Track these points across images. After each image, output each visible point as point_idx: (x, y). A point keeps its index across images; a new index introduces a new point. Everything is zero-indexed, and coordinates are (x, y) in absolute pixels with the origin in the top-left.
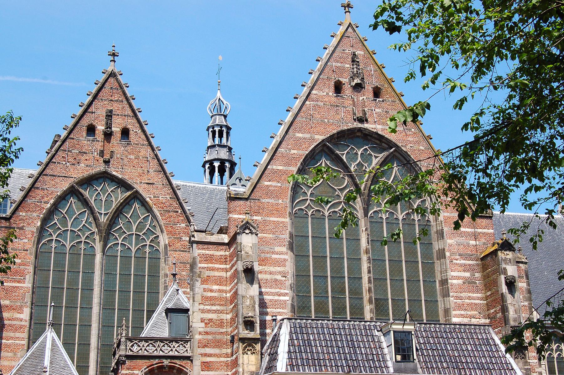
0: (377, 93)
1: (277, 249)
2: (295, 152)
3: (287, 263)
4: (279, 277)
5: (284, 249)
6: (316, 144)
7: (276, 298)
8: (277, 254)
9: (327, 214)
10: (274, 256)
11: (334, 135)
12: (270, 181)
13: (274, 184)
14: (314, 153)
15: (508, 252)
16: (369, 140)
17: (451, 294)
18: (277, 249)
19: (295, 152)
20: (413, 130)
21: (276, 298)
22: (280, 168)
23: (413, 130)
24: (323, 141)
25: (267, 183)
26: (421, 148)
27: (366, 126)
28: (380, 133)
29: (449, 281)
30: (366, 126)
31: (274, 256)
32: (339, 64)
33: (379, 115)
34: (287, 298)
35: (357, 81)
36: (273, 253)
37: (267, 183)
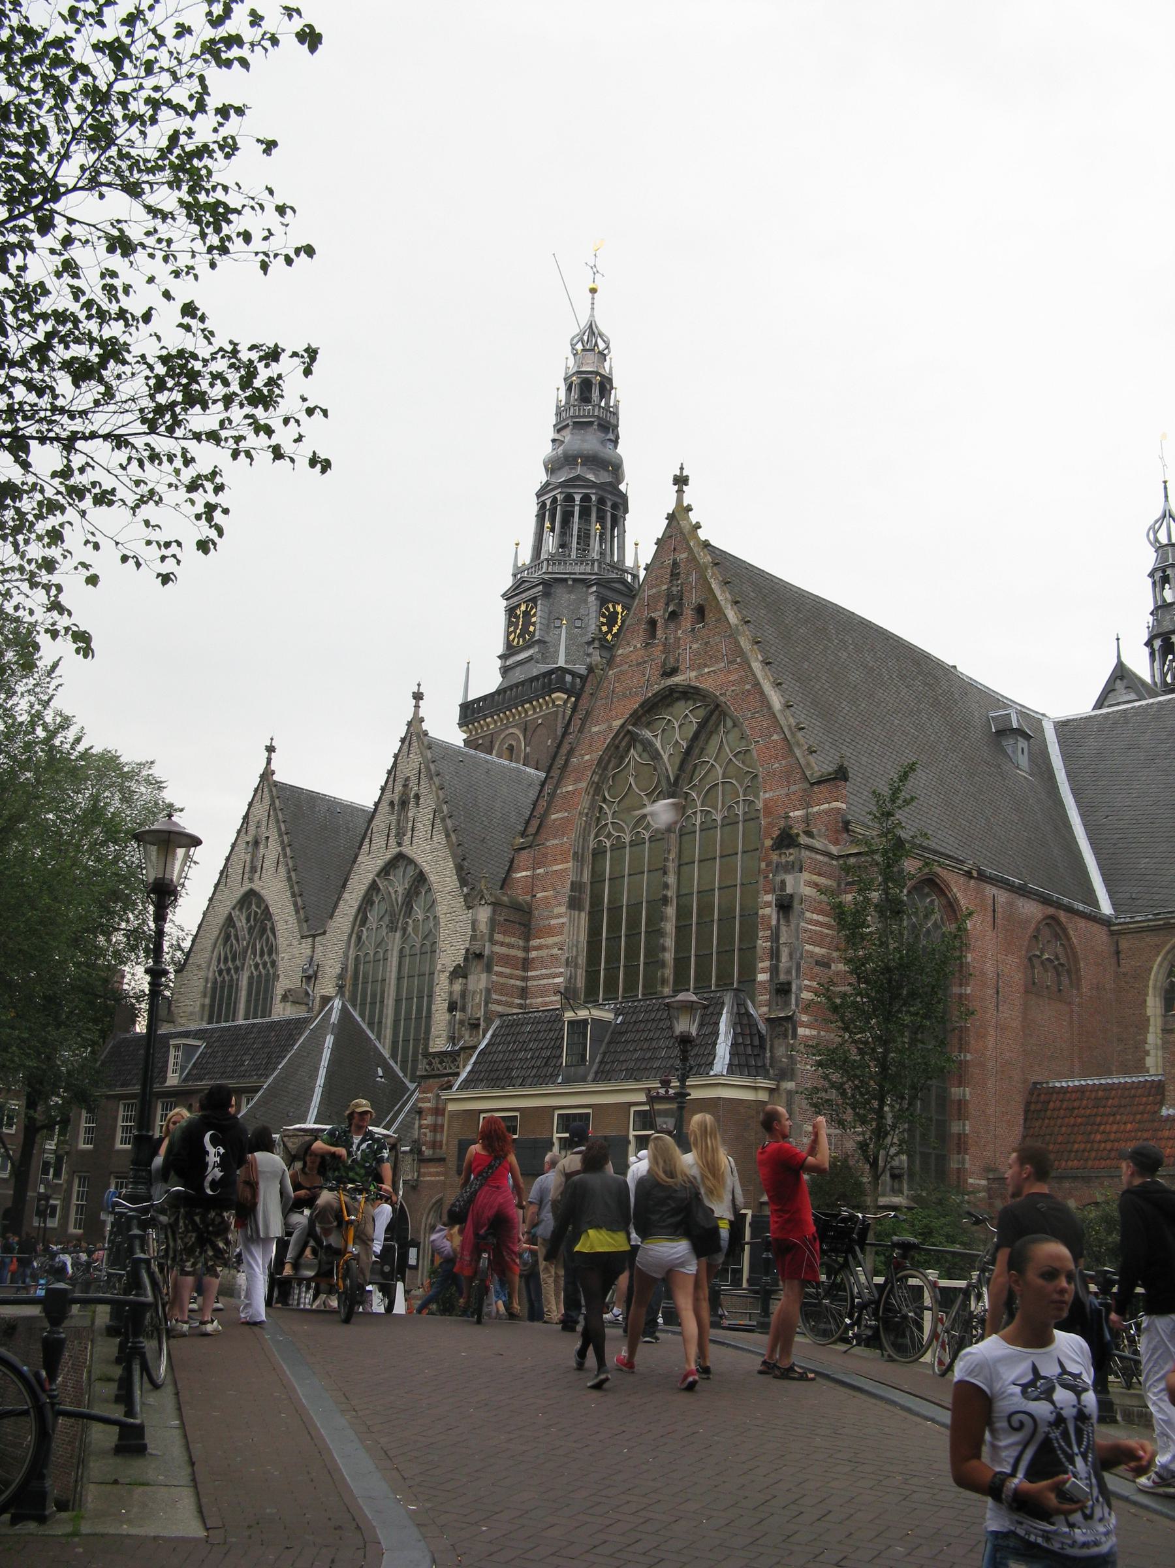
0: (700, 611)
1: (557, 910)
2: (587, 757)
3: (566, 929)
4: (555, 951)
5: (563, 909)
6: (612, 735)
7: (551, 981)
8: (557, 917)
9: (628, 840)
10: (553, 922)
11: (636, 711)
12: (557, 812)
13: (560, 815)
14: (617, 747)
15: (791, 851)
16: (689, 699)
17: (761, 934)
18: (557, 910)
19: (587, 757)
20: (738, 660)
21: (551, 981)
22: (570, 788)
23: (738, 660)
24: (623, 726)
25: (553, 817)
26: (748, 687)
27: (677, 679)
28: (693, 684)
29: (761, 912)
30: (677, 679)
31: (553, 922)
32: (654, 590)
33: (697, 653)
34: (561, 980)
35: (671, 609)
36: (552, 918)
37: (553, 817)
